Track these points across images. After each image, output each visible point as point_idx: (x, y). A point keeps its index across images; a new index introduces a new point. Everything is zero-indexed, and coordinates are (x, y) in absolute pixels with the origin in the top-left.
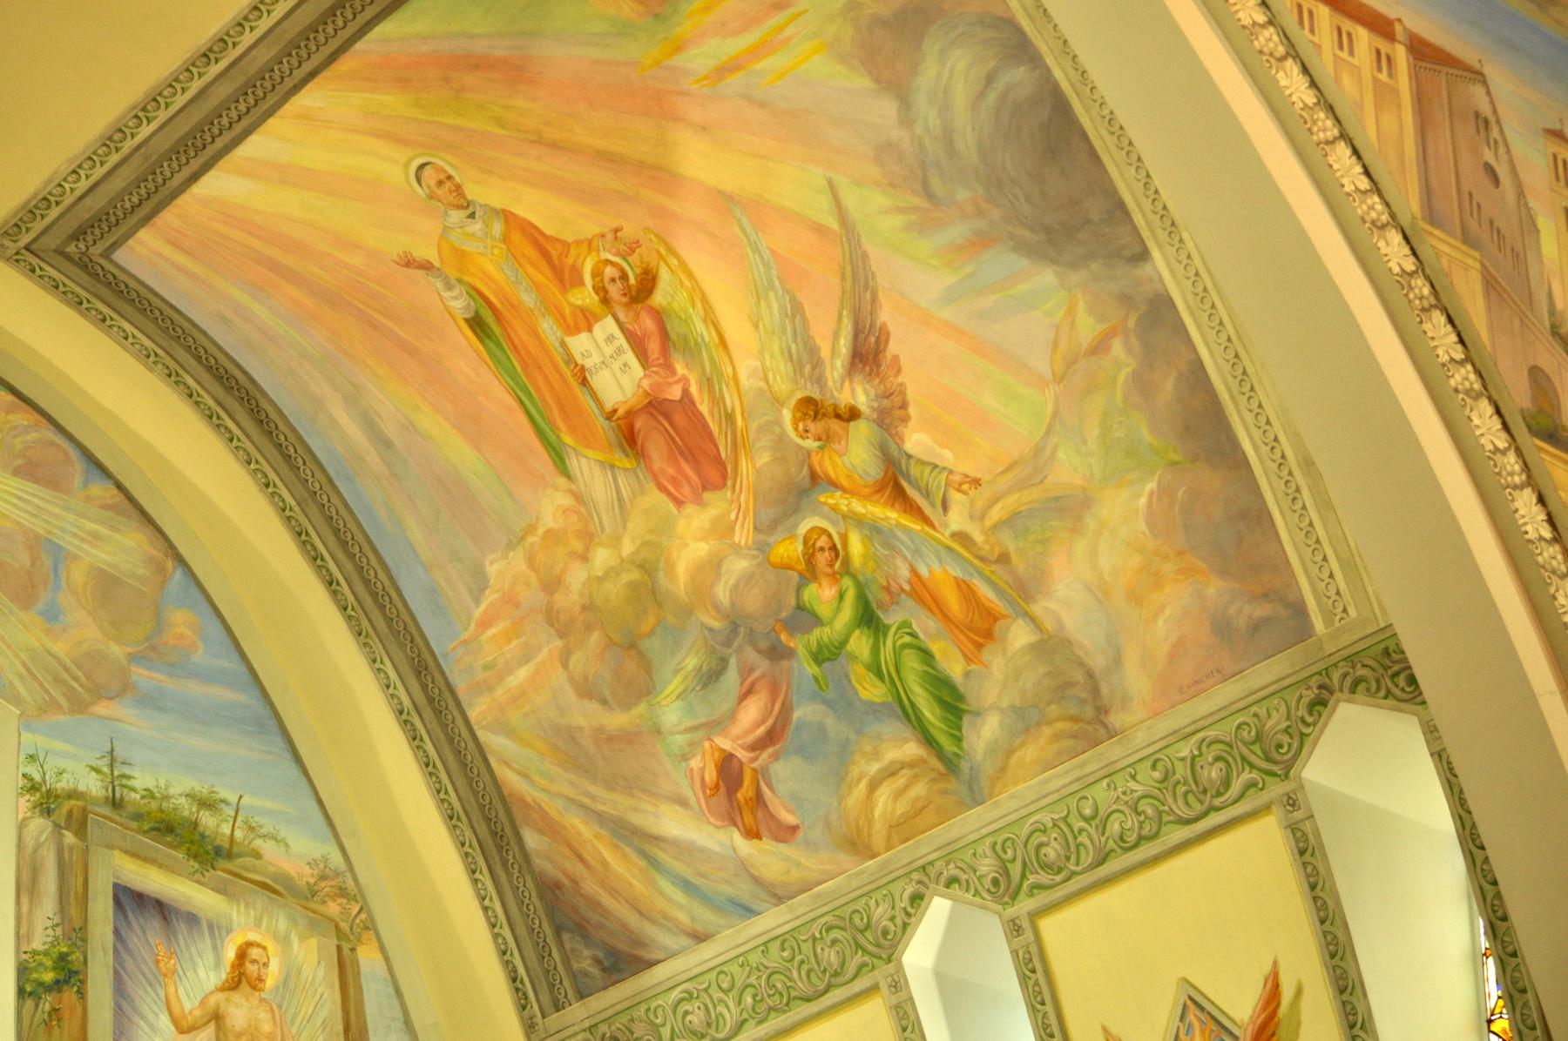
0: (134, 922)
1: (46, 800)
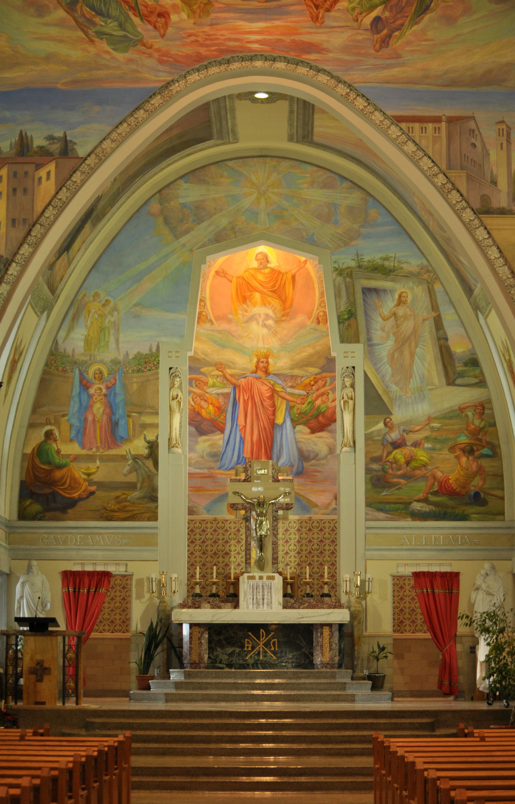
0: (368, 295)
1: (340, 272)
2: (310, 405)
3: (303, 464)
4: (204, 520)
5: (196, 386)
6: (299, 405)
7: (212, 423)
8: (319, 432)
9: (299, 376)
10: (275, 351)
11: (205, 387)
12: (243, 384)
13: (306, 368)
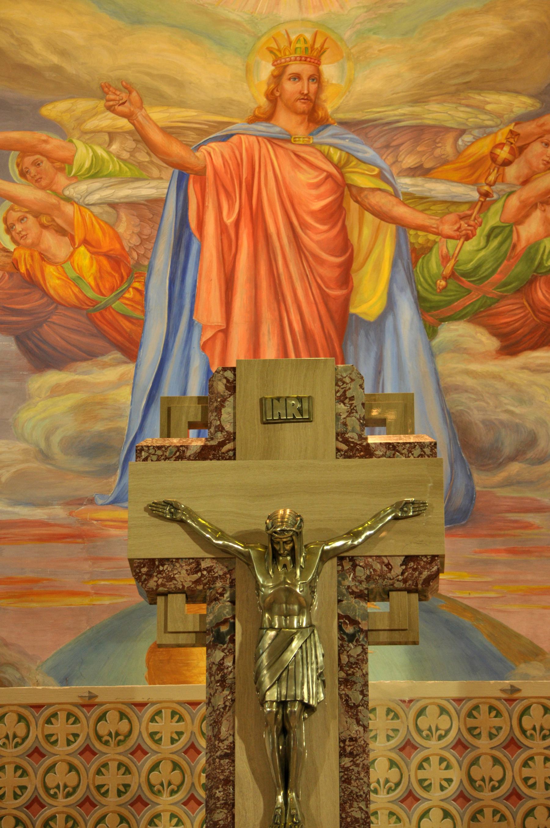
2: (494, 243)
3: (470, 477)
4: (38, 707)
5: (23, 174)
6: (451, 243)
7: (89, 317)
8: (534, 347)
9: (448, 129)
10: (347, 34)
11: (61, 180)
12: (219, 162)
13: (477, 98)
